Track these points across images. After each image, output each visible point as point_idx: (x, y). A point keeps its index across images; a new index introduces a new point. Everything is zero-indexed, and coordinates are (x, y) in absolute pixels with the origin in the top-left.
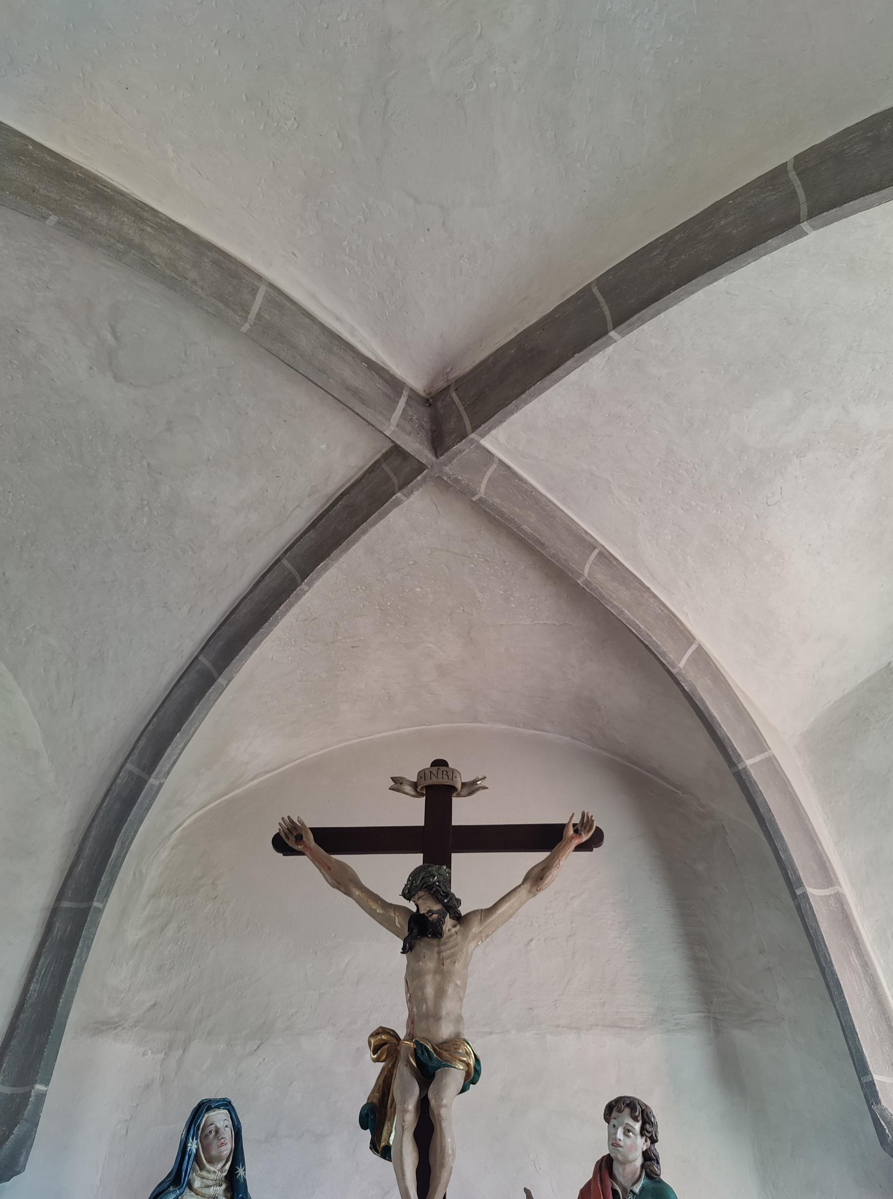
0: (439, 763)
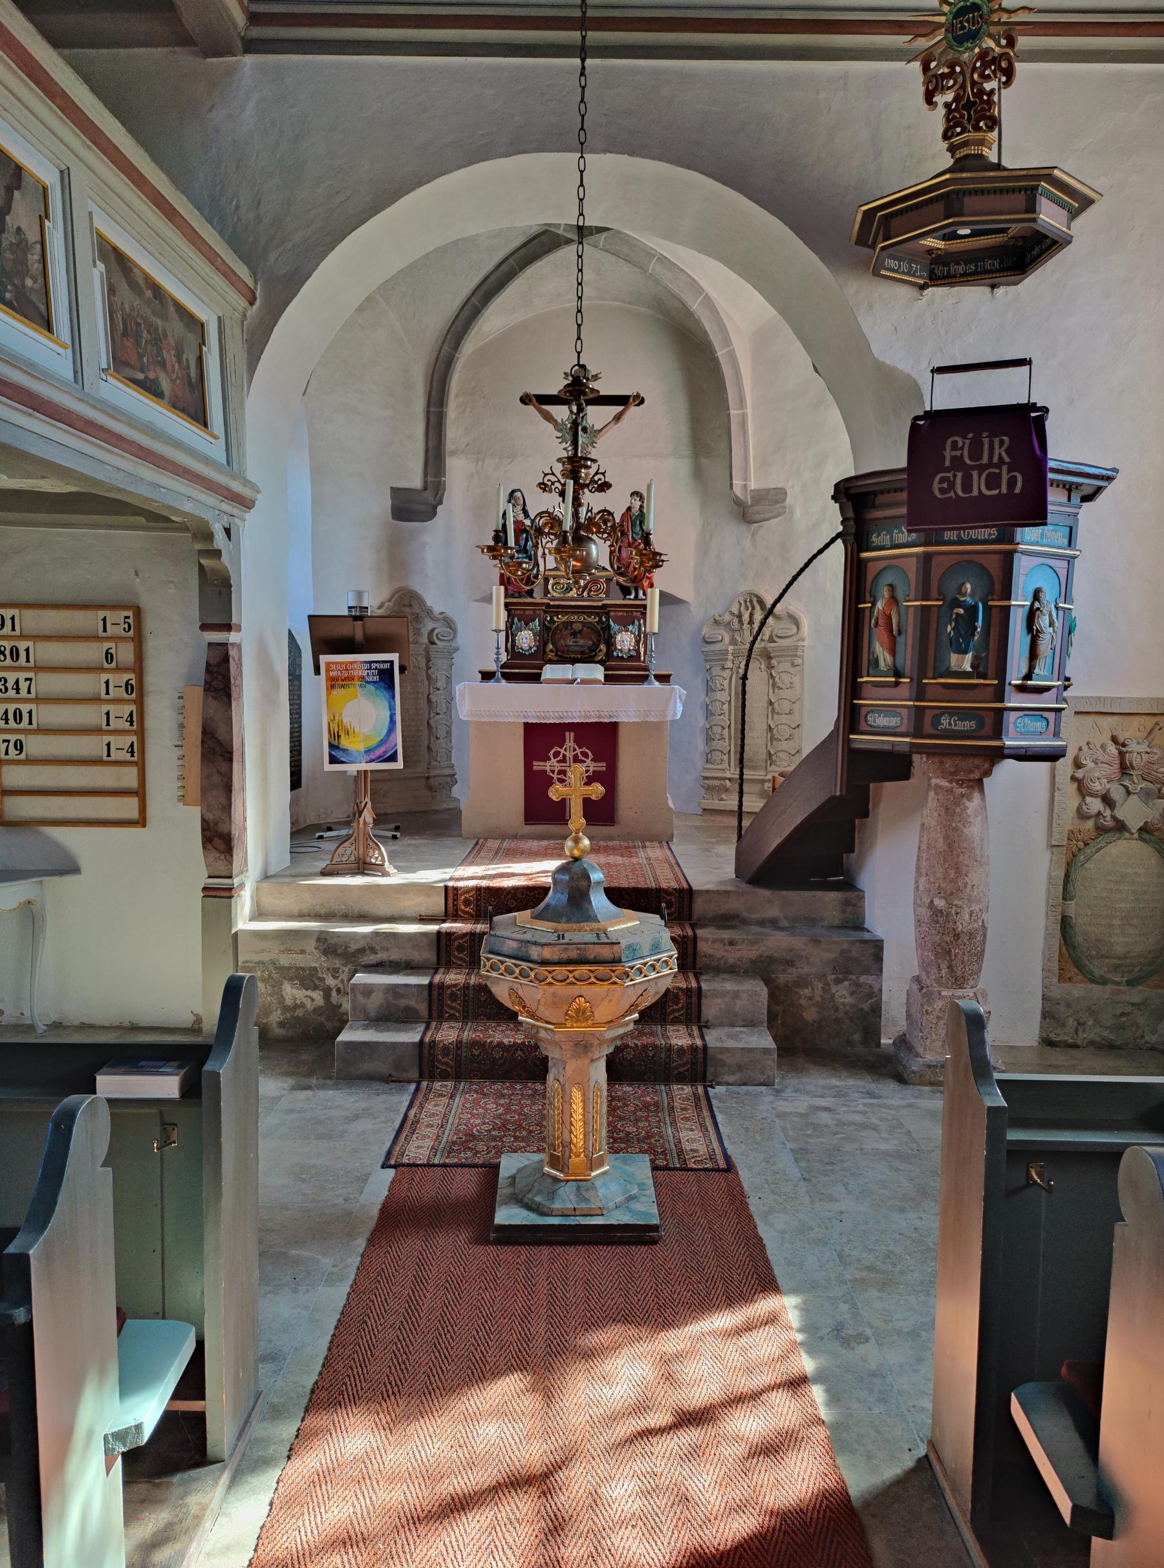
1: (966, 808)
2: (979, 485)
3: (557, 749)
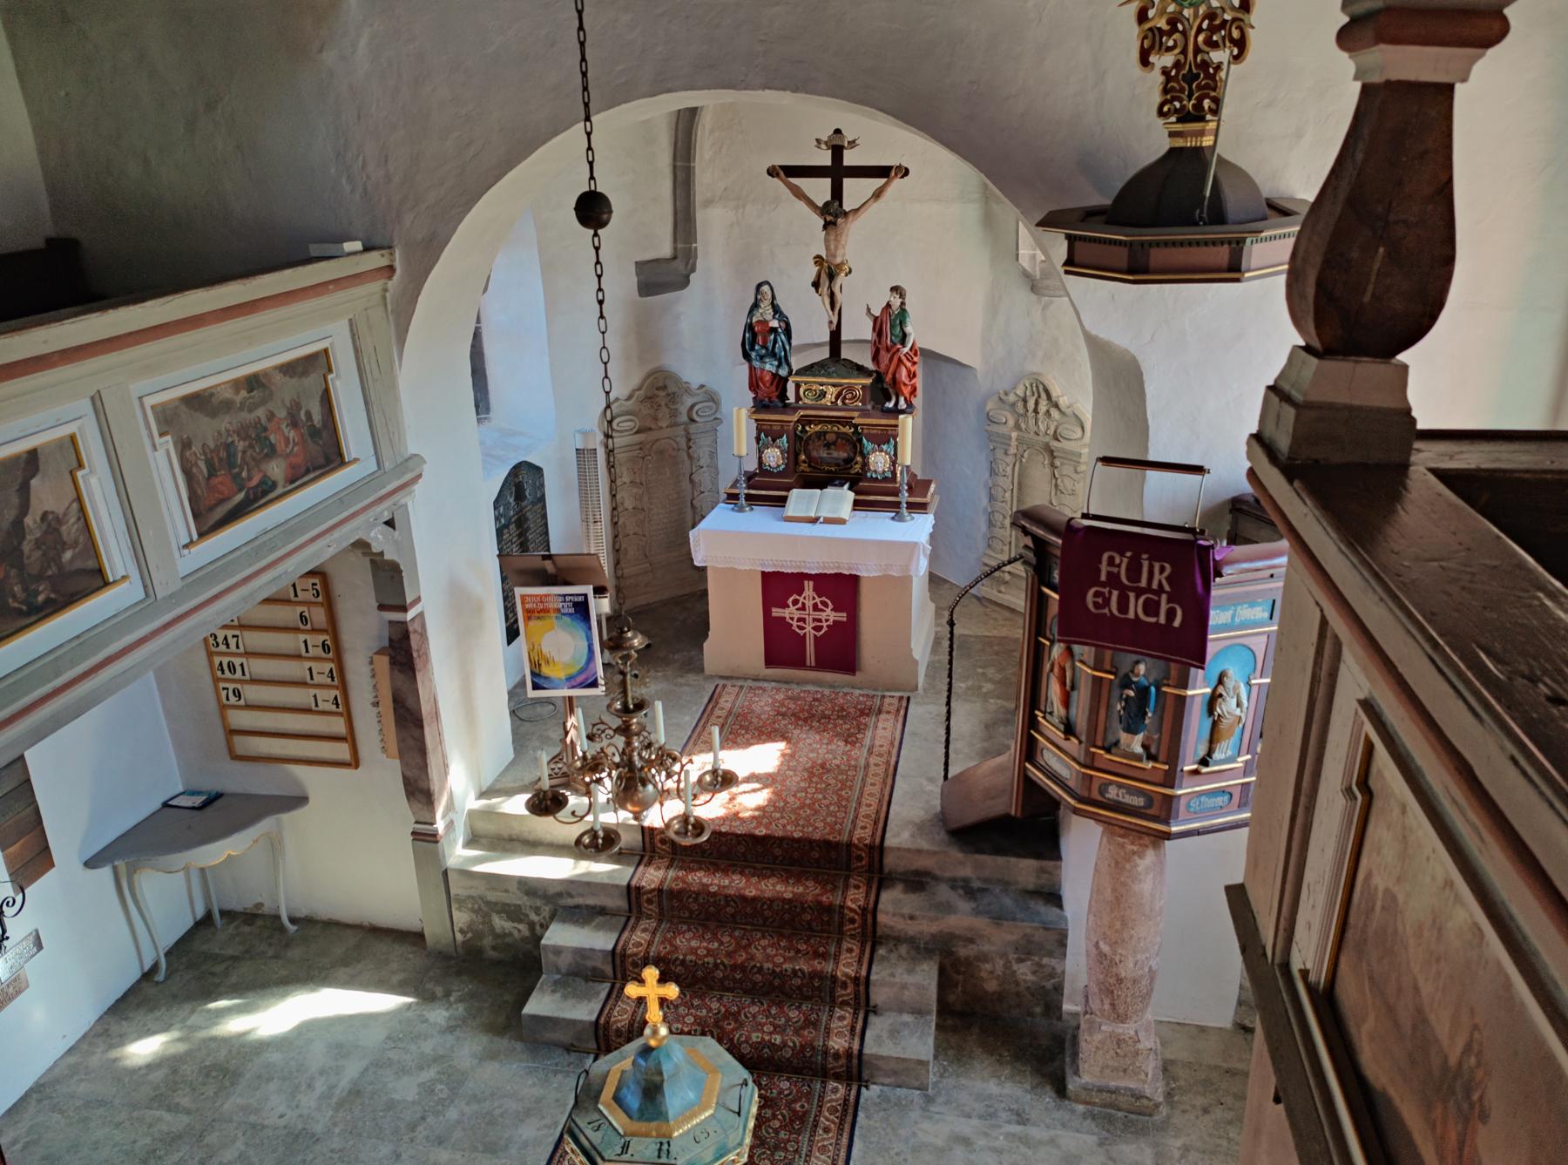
0: (838, 131)
1: (1136, 865)
2: (1136, 608)
3: (795, 596)
